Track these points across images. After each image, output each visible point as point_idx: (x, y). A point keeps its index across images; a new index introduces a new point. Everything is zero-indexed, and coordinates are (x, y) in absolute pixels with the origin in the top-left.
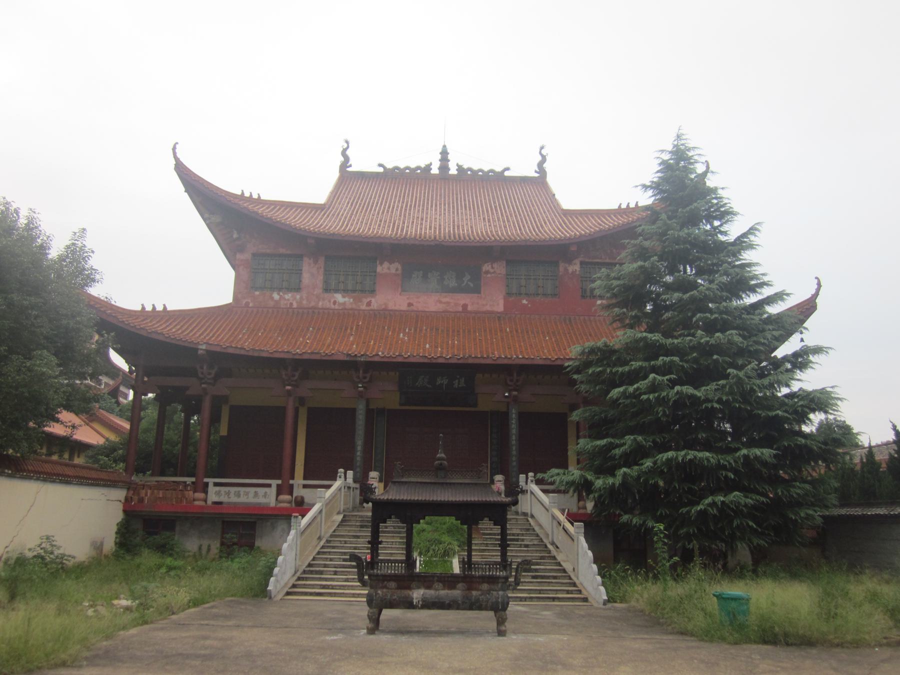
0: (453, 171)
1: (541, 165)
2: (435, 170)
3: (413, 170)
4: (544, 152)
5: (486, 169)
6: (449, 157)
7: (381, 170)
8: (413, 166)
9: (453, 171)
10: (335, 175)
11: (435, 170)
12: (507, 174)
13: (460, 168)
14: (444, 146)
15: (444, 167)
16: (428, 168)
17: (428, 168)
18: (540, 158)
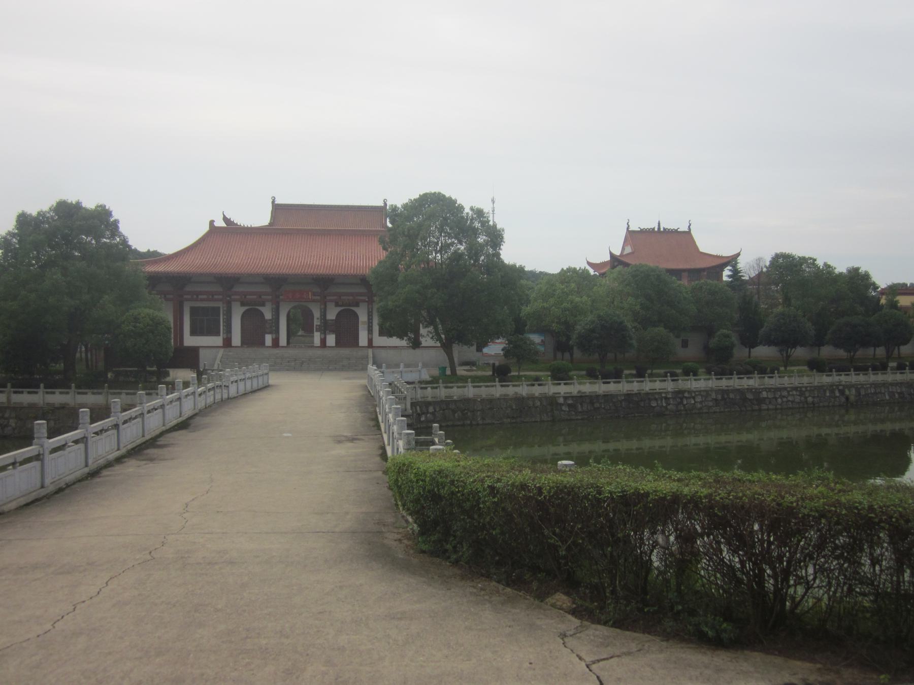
0: (662, 230)
1: (689, 227)
2: (656, 229)
4: (690, 222)
5: (672, 228)
6: (661, 225)
7: (639, 229)
8: (649, 228)
9: (662, 230)
11: (656, 229)
12: (679, 230)
13: (664, 228)
14: (659, 221)
15: (659, 228)
16: (654, 229)
17: (654, 229)
18: (689, 225)
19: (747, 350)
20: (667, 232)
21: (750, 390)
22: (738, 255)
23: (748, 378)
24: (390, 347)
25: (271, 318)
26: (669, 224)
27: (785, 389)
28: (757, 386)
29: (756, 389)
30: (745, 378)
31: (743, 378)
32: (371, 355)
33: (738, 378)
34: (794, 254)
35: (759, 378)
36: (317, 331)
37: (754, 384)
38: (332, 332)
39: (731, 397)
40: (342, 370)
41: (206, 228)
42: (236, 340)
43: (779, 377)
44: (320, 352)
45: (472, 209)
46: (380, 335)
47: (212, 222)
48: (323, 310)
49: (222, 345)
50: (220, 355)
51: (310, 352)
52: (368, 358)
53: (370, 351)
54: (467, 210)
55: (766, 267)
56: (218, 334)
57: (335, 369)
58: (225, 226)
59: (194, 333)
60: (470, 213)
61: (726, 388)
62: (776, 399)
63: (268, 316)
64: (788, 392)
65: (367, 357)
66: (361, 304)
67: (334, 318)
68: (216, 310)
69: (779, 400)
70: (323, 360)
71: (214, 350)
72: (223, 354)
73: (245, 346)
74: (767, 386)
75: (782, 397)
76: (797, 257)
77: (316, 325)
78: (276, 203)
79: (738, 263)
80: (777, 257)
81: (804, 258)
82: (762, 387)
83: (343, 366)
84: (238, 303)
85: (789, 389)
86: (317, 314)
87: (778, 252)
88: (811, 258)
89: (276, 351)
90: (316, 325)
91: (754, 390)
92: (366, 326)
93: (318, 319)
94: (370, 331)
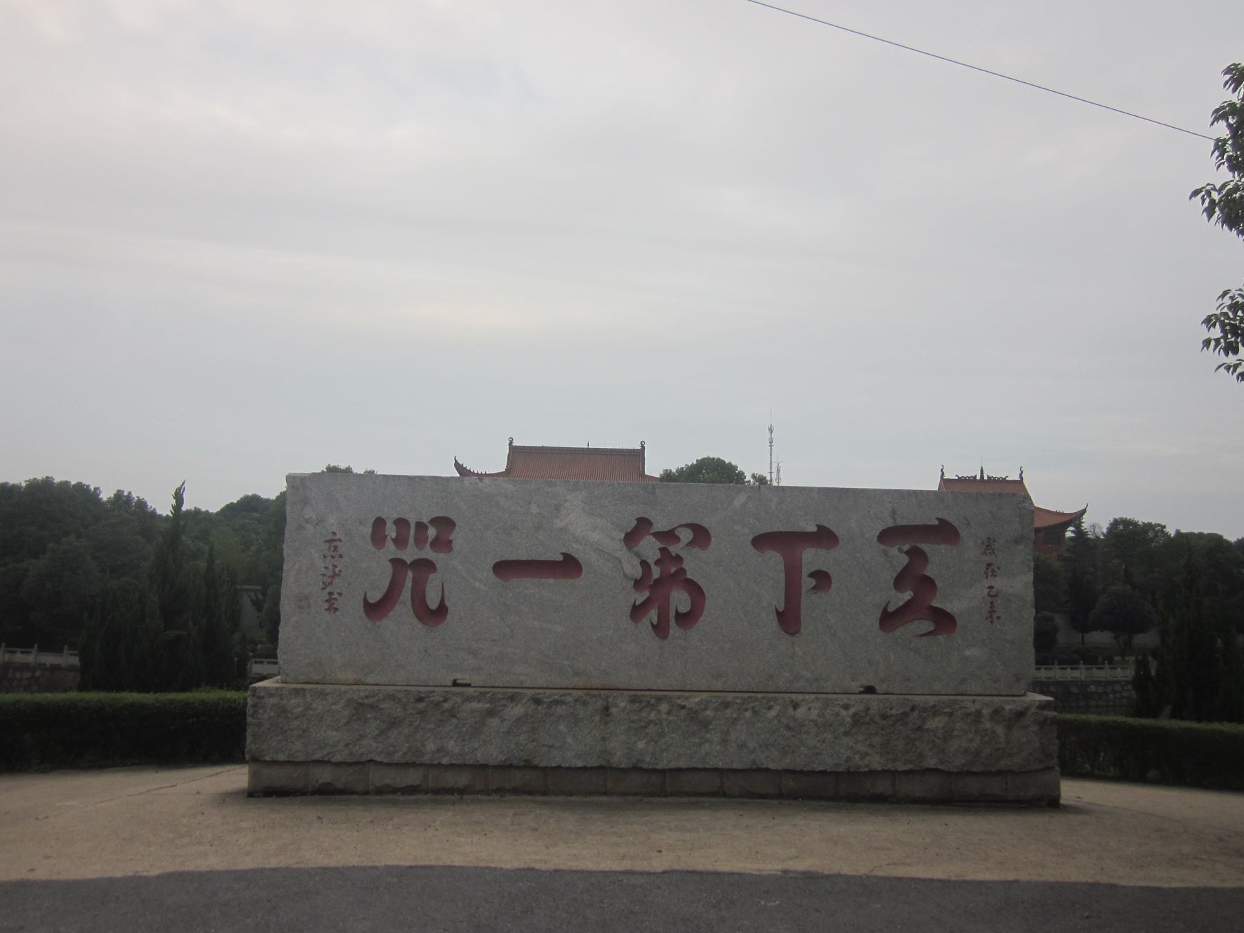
0: (986, 478)
1: (1021, 475)
2: (978, 478)
3: (969, 478)
7: (957, 478)
9: (986, 478)
10: (940, 479)
11: (978, 478)
13: (988, 477)
14: (982, 468)
15: (982, 476)
16: (976, 476)
17: (976, 476)
19: (1081, 635)
20: (992, 480)
21: (1075, 683)
22: (1084, 511)
23: (1071, 669)
26: (995, 471)
27: (1118, 682)
28: (1083, 677)
29: (1082, 682)
30: (1069, 669)
31: (1066, 669)
33: (1061, 669)
34: (1136, 520)
35: (1087, 669)
37: (1079, 676)
39: (1052, 690)
43: (1110, 668)
45: (753, 476)
54: (748, 478)
55: (1103, 533)
58: (459, 475)
60: (752, 480)
61: (1046, 680)
62: (1107, 694)
64: (1122, 686)
69: (1111, 696)
74: (1095, 679)
75: (1114, 692)
76: (1140, 523)
78: (514, 444)
79: (1083, 523)
80: (1116, 523)
81: (1150, 525)
82: (1090, 679)
85: (1123, 683)
87: (1117, 517)
88: (1159, 525)
91: (1079, 683)
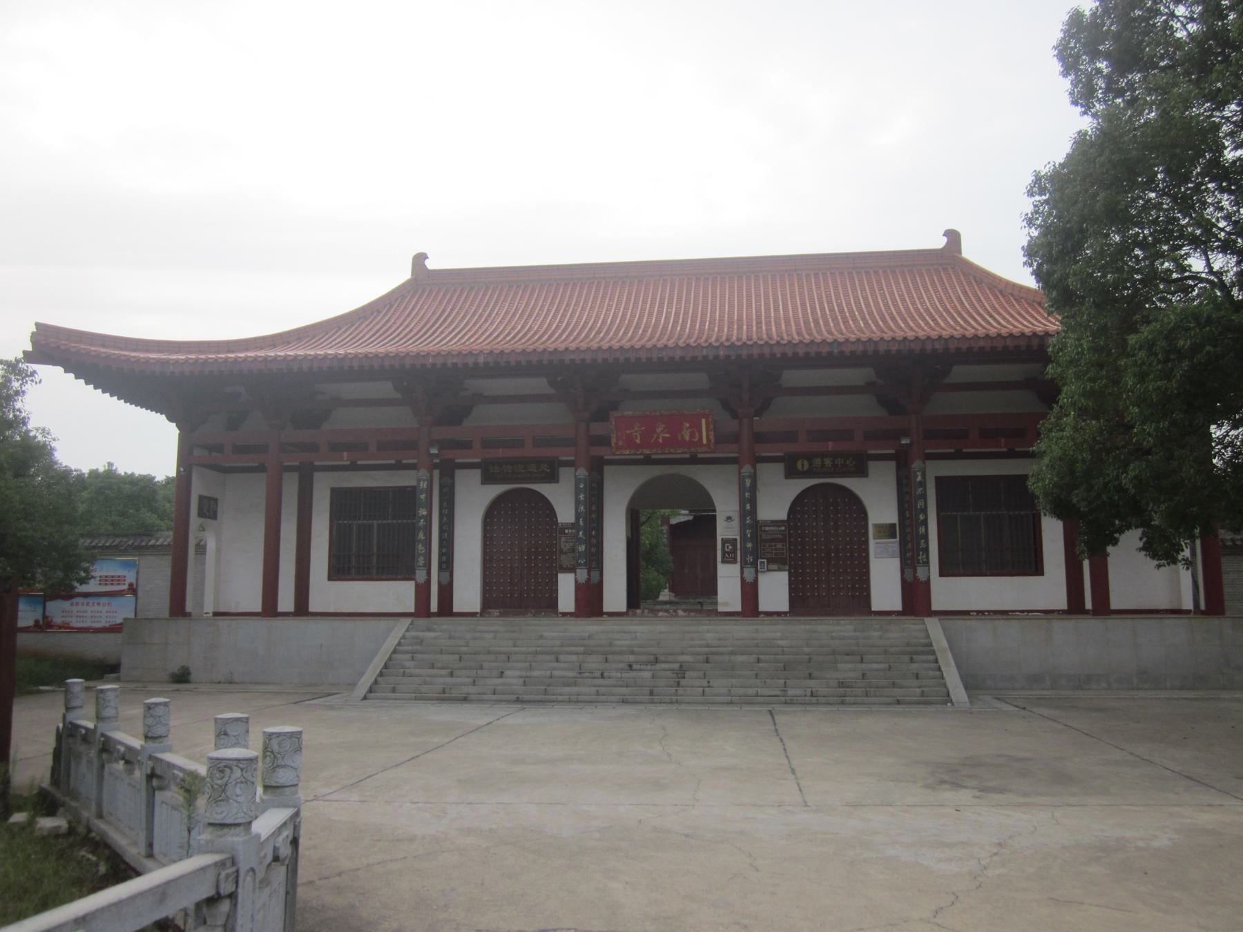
24: (982, 612)
25: (572, 519)
32: (945, 644)
36: (723, 562)
38: (777, 562)
40: (843, 703)
41: (403, 274)
42: (468, 594)
44: (743, 630)
46: (942, 574)
47: (419, 259)
48: (748, 482)
49: (413, 610)
50: (391, 642)
51: (708, 632)
52: (933, 653)
53: (933, 626)
56: (408, 575)
57: (813, 700)
59: (338, 571)
63: (566, 513)
65: (928, 648)
66: (873, 466)
67: (783, 515)
68: (406, 499)
70: (758, 661)
71: (383, 623)
72: (404, 637)
73: (496, 612)
77: (724, 541)
83: (841, 684)
84: (476, 474)
86: (726, 508)
89: (589, 627)
90: (724, 541)
92: (894, 544)
93: (729, 518)
94: (911, 557)
